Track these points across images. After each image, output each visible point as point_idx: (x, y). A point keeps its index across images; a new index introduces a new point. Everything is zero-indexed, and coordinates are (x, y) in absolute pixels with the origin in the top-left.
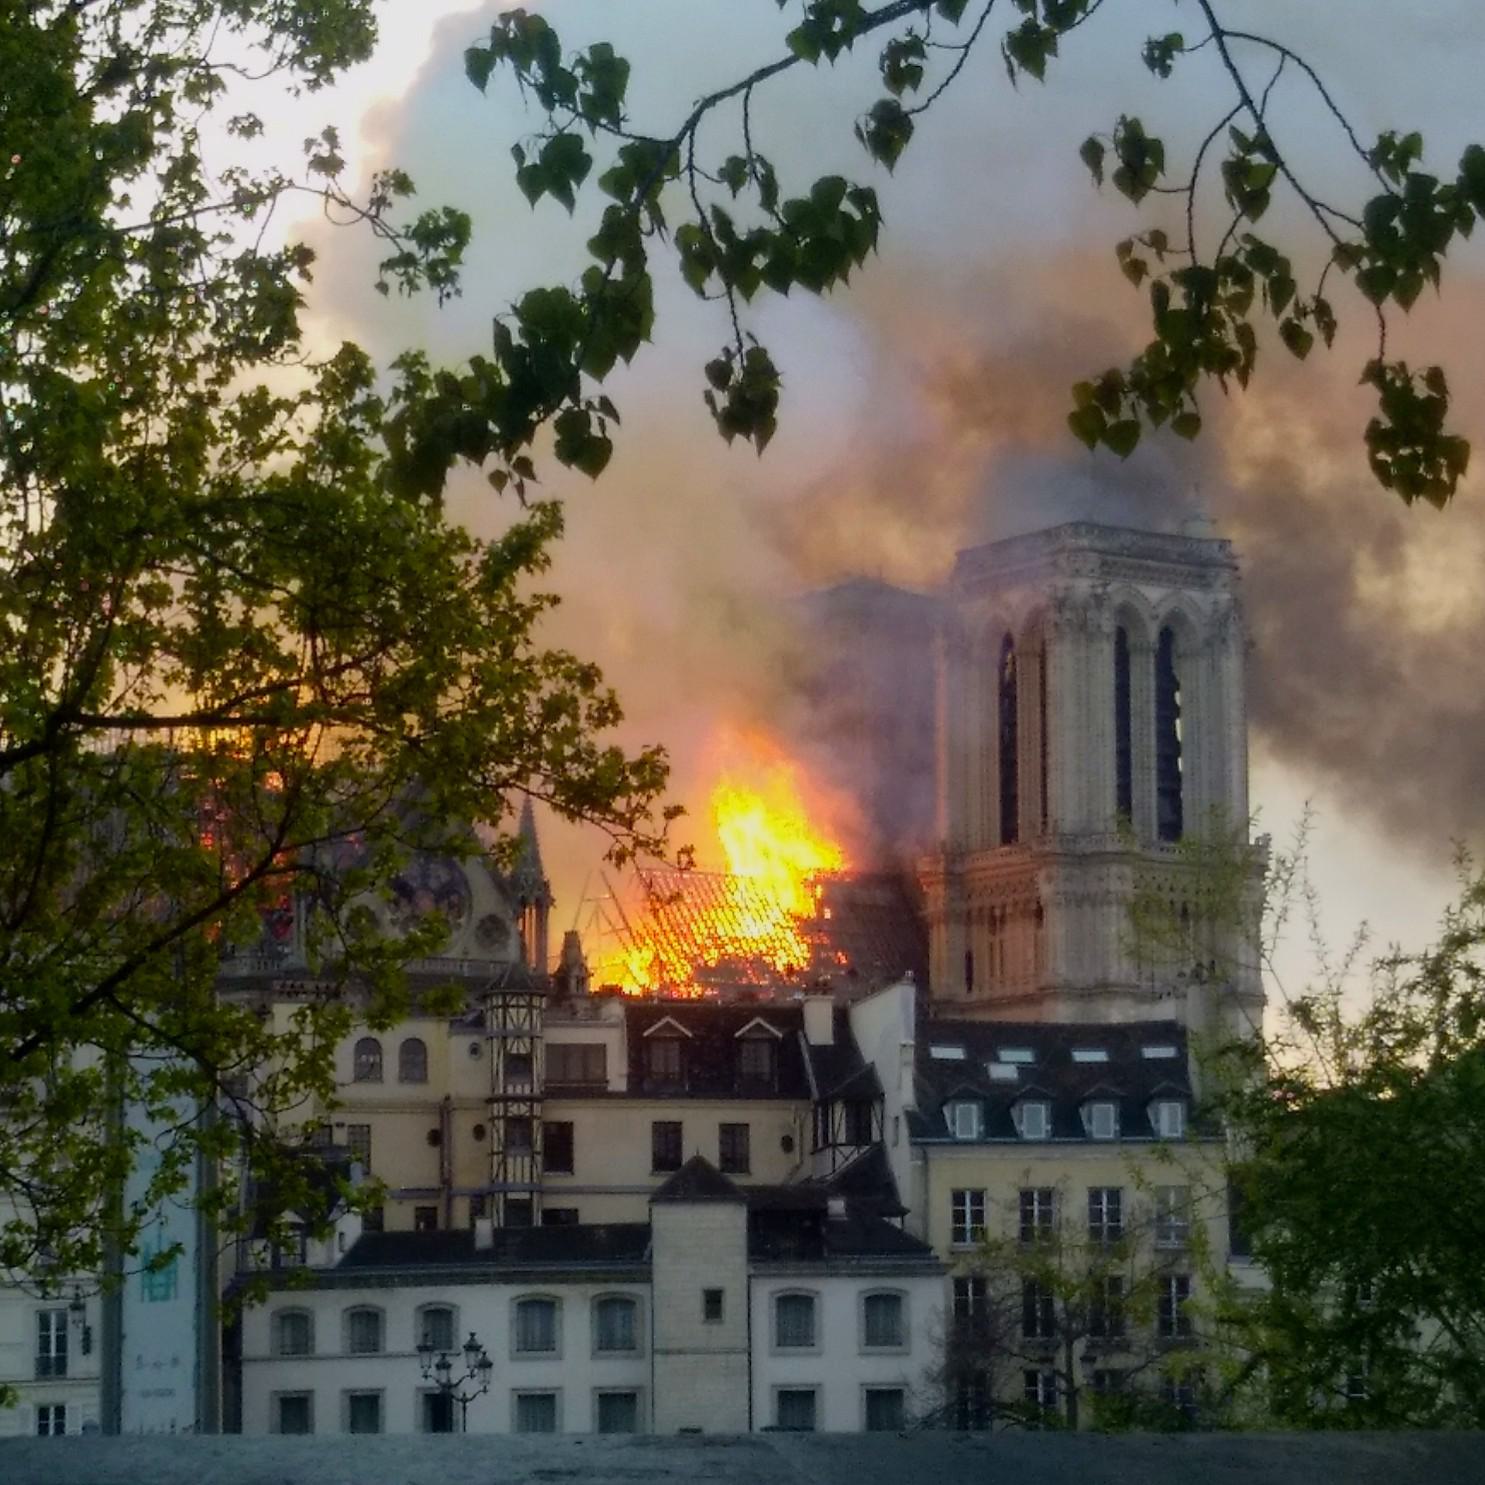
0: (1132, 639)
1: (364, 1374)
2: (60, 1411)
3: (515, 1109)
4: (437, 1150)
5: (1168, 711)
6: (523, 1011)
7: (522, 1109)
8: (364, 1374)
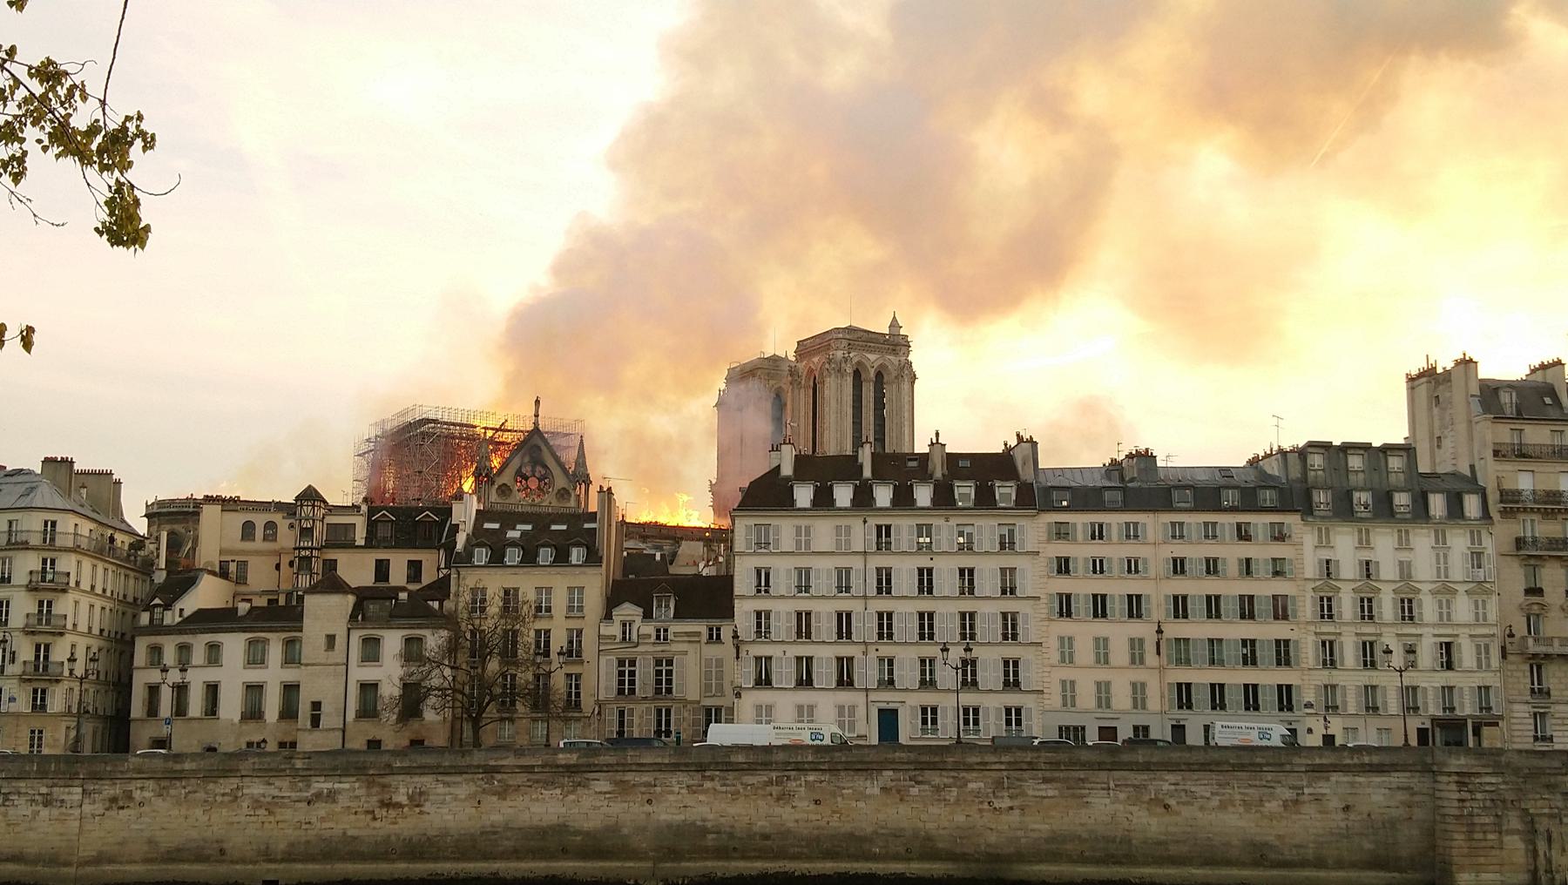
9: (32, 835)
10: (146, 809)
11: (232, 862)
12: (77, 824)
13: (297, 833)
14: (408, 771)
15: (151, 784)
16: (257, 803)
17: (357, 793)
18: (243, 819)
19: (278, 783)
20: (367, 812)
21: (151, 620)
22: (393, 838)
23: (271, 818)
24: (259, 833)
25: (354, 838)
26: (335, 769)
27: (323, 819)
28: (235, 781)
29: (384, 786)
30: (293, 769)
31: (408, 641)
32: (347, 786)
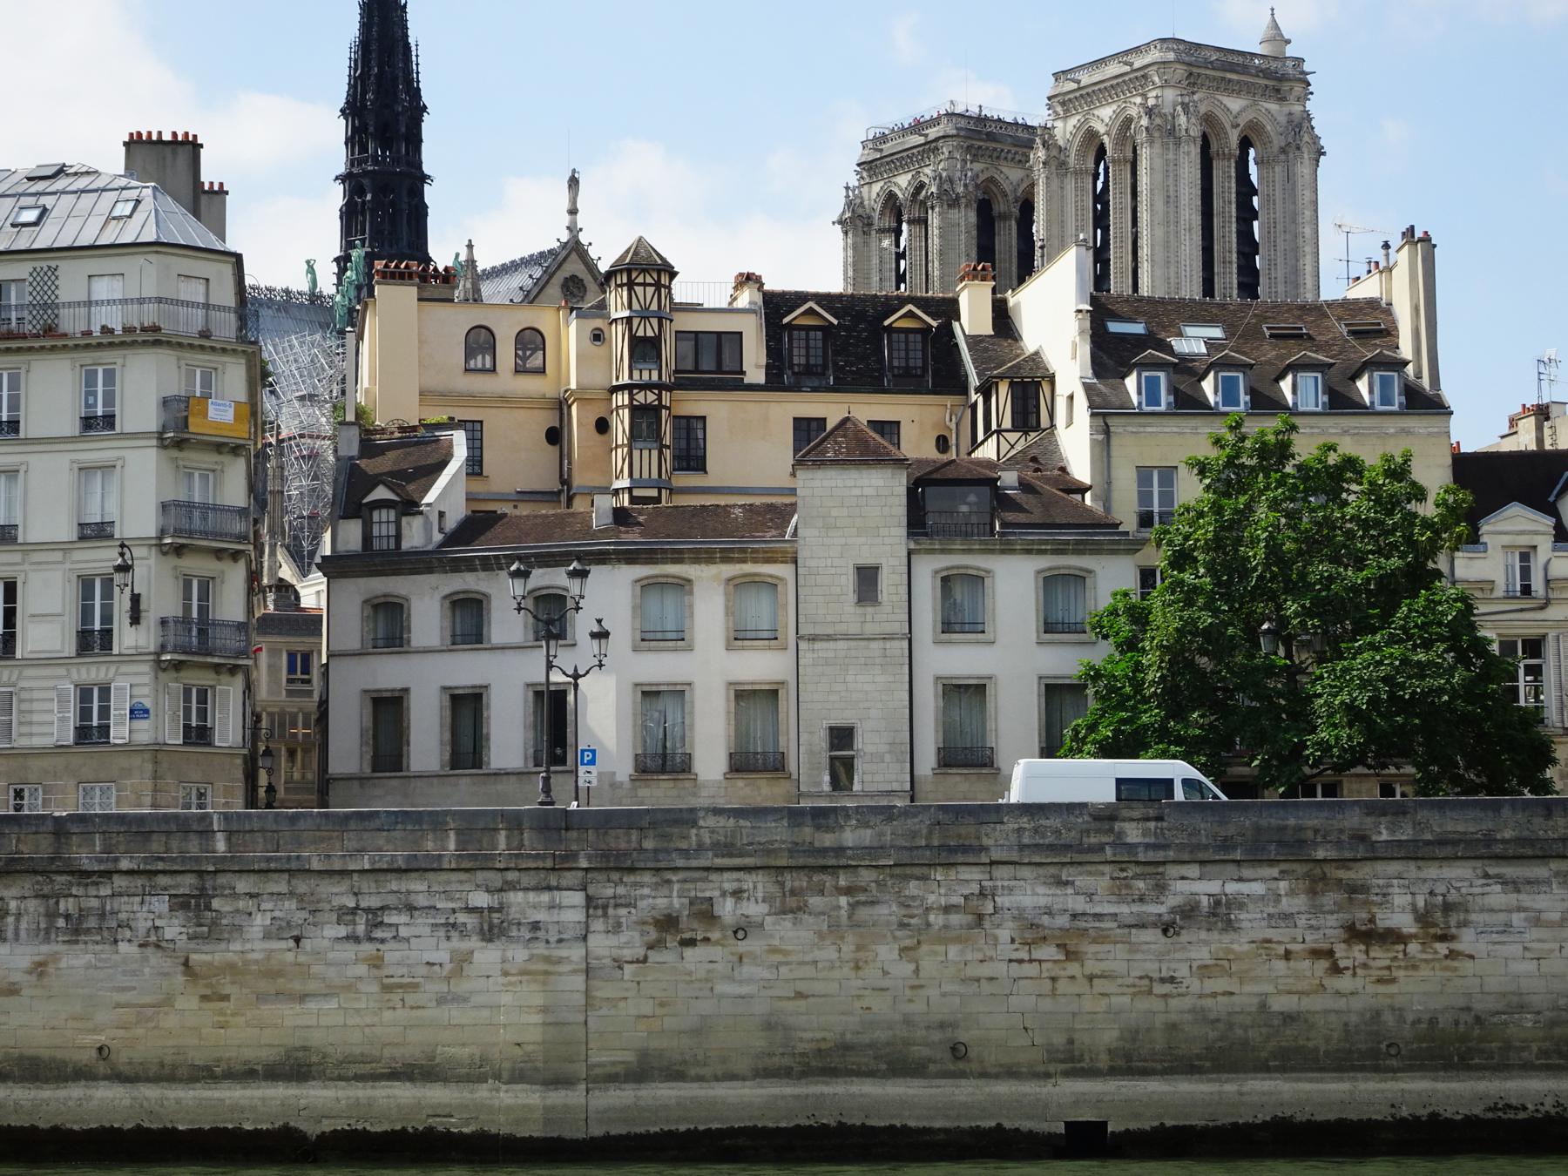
0: (1214, 147)
1: (466, 669)
2: (105, 692)
3: (640, 397)
4: (555, 450)
5: (1247, 214)
6: (650, 290)
7: (651, 397)
8: (466, 669)
9: (455, 1014)
10: (752, 945)
11: (984, 1075)
12: (579, 982)
13: (1143, 1004)
14: (1415, 852)
15: (759, 883)
16: (1032, 932)
17: (1286, 904)
18: (1000, 969)
19: (1083, 881)
20: (1316, 954)
21: (367, 538)
22: (1389, 1019)
23: (1073, 968)
24: (1046, 1004)
25: (1289, 1018)
26: (1226, 844)
27: (1204, 971)
28: (974, 874)
29: (1353, 889)
30: (1120, 844)
31: (1051, 583)
32: (1257, 888)
